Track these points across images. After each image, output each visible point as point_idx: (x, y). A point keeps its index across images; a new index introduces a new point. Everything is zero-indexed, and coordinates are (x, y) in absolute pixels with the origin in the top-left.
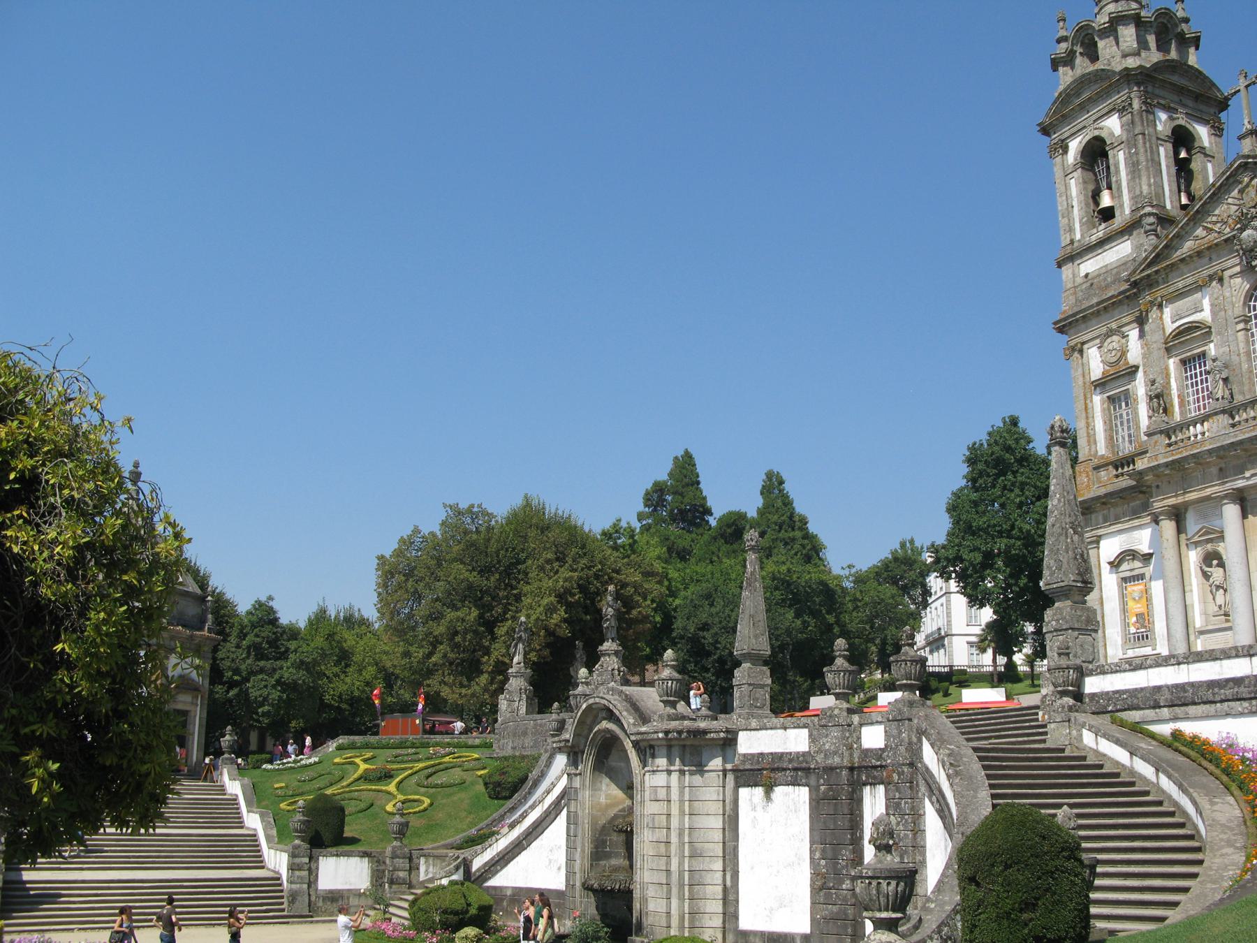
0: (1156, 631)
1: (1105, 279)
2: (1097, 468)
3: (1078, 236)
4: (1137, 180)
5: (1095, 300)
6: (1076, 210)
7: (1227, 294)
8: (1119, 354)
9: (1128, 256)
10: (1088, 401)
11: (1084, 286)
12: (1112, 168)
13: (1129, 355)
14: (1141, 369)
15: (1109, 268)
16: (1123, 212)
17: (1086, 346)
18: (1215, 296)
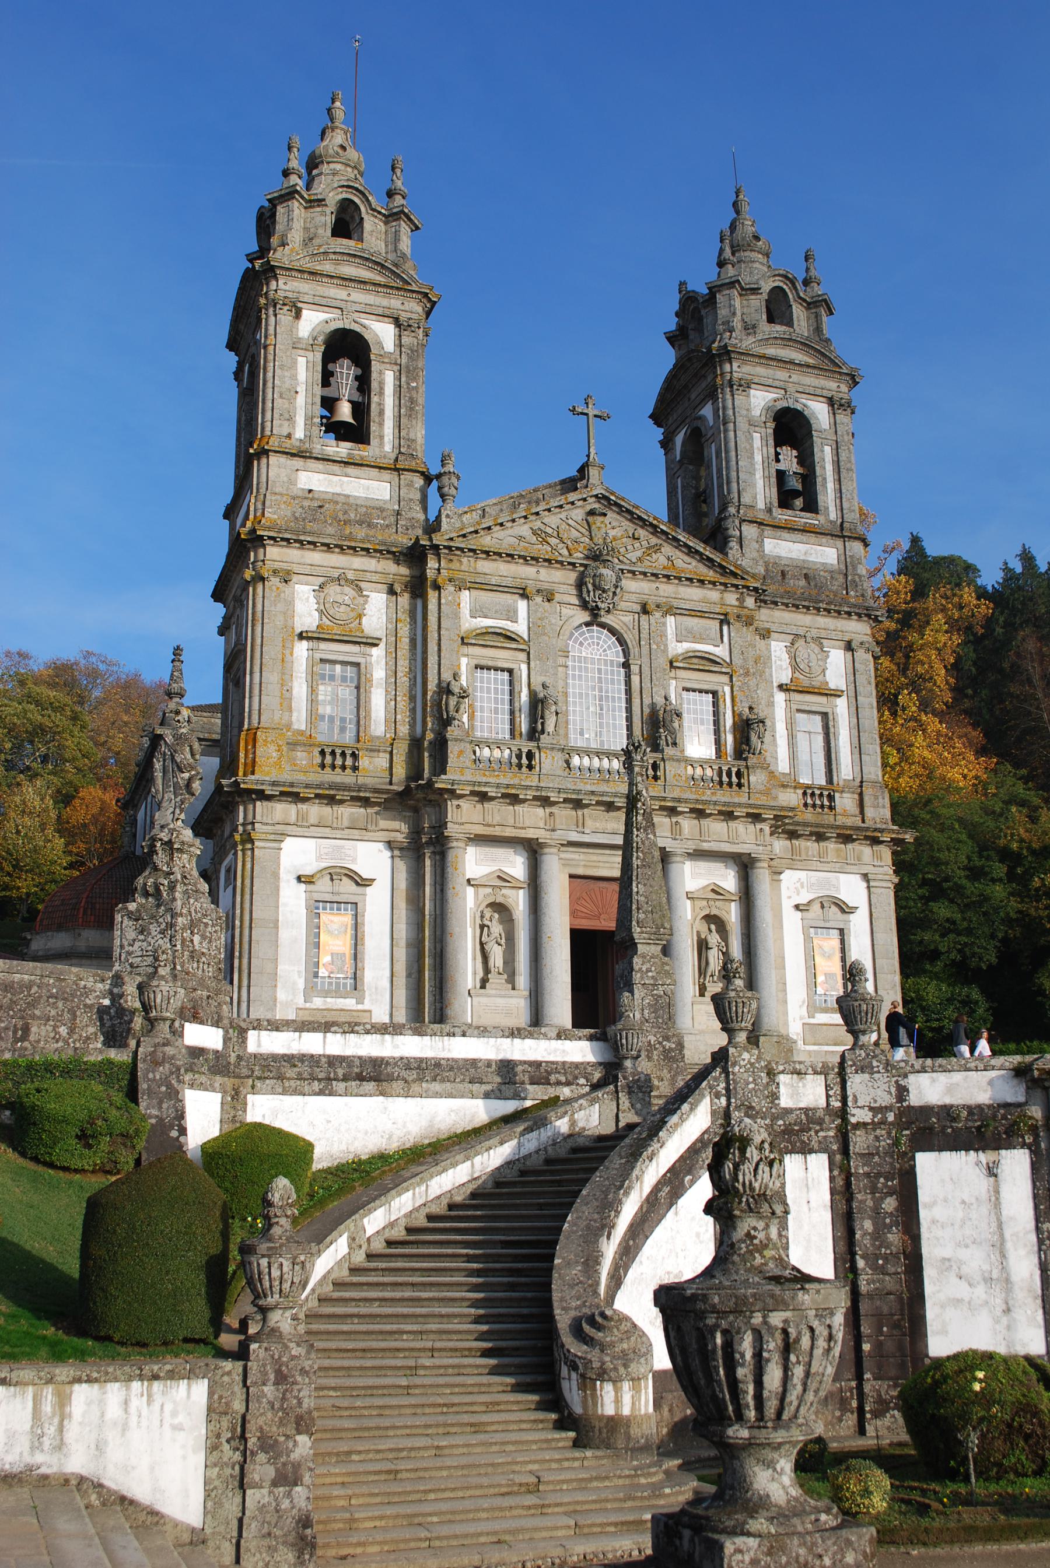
0: (366, 980)
1: (345, 513)
2: (293, 745)
3: (299, 433)
4: (414, 422)
5: (330, 530)
6: (301, 400)
7: (553, 621)
8: (352, 615)
9: (385, 502)
10: (287, 652)
11: (306, 503)
12: (374, 385)
13: (364, 620)
14: (382, 645)
15: (352, 501)
16: (382, 444)
17: (295, 578)
18: (539, 615)
